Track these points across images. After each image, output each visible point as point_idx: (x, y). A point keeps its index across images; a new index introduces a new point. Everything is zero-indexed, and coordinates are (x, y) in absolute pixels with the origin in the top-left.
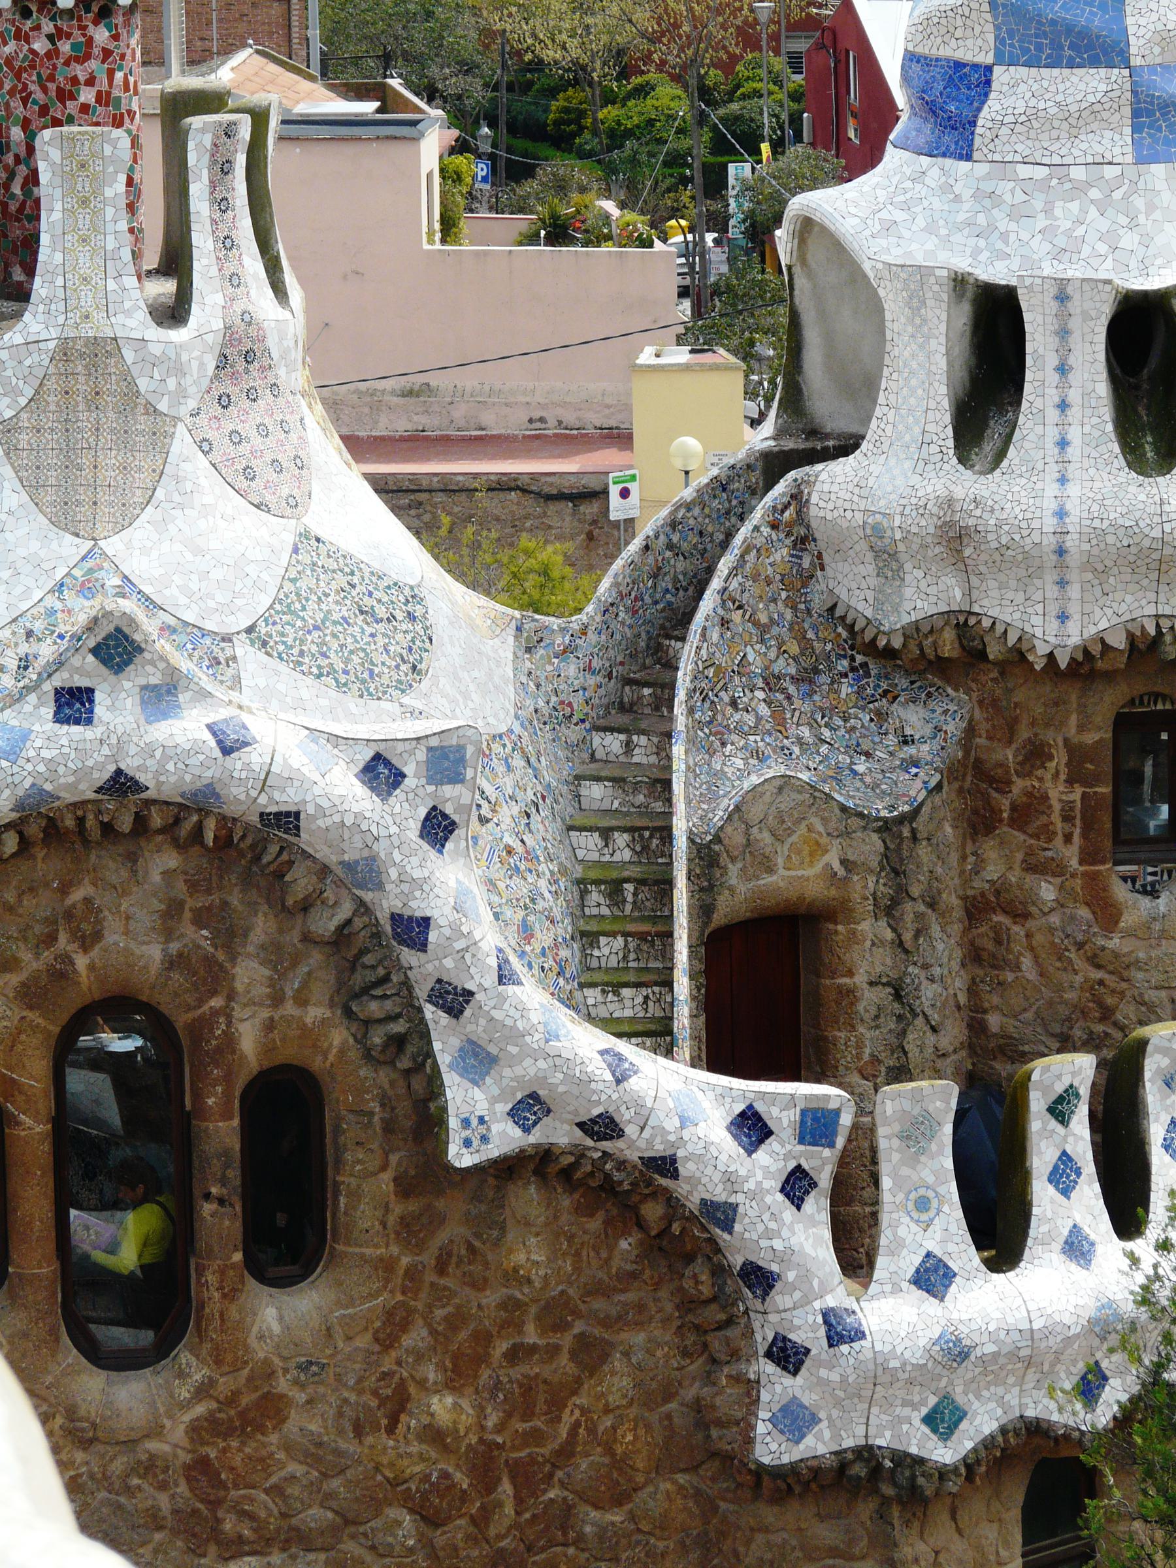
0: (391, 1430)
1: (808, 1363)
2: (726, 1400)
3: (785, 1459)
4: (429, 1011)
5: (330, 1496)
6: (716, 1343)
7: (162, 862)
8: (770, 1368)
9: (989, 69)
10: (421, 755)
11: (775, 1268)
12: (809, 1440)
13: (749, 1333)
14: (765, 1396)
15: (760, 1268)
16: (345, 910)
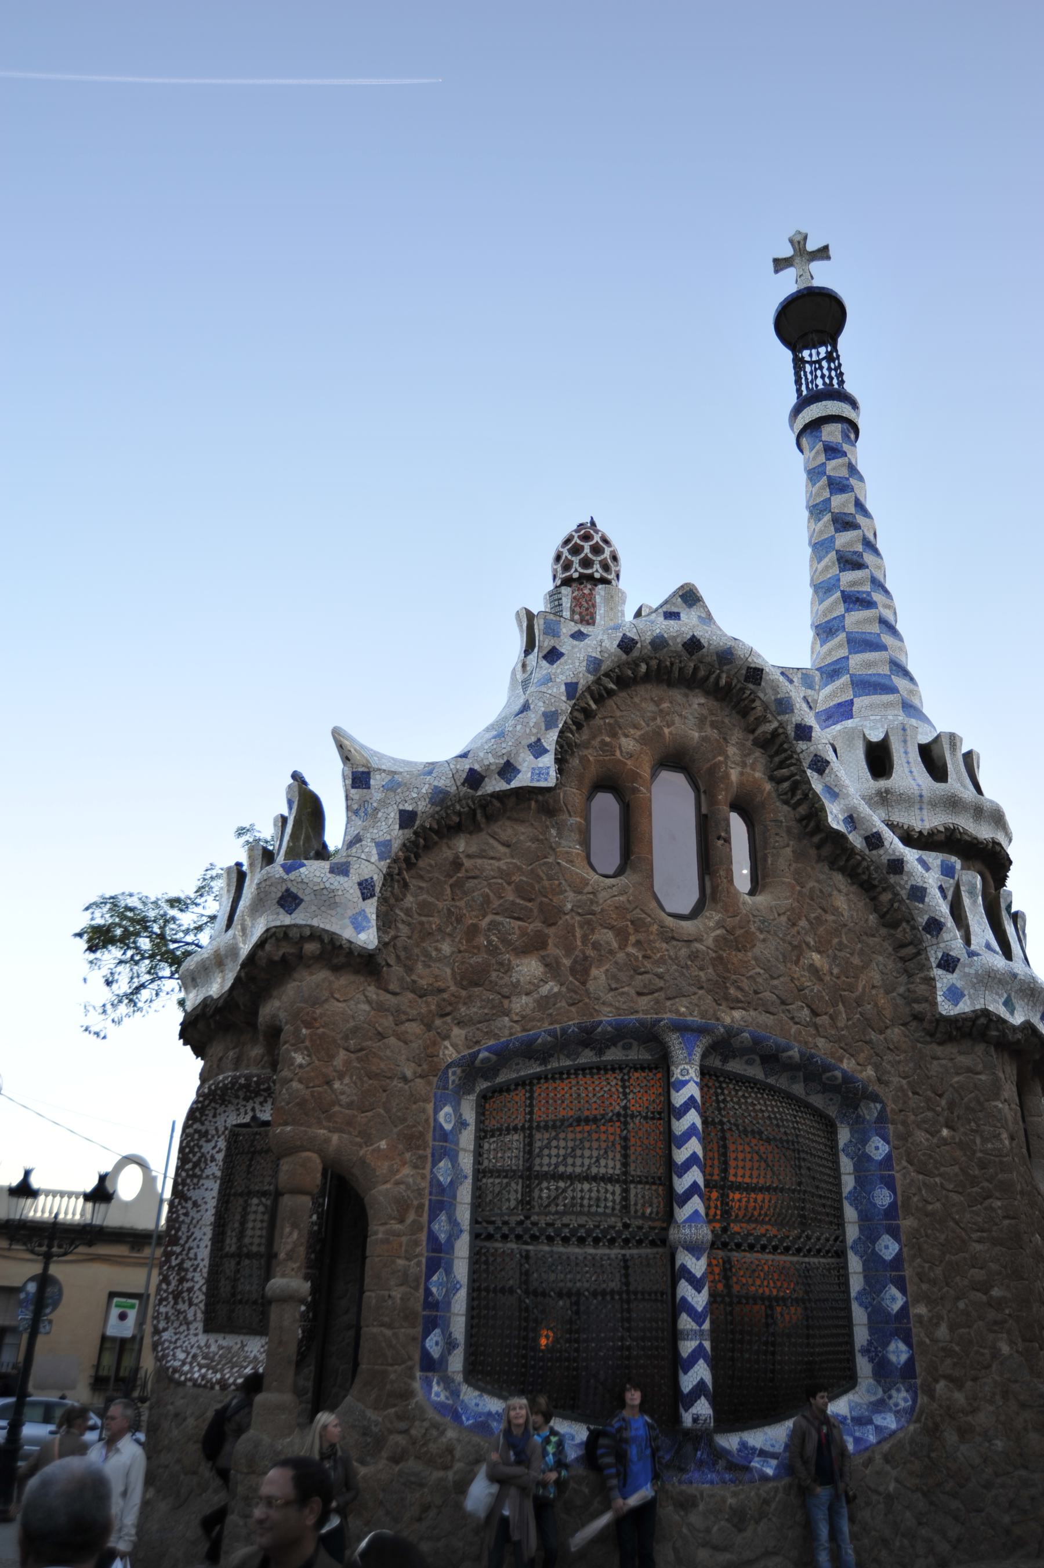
0: (797, 963)
1: (959, 966)
2: (921, 989)
3: (952, 1013)
4: (809, 772)
5: (775, 987)
6: (910, 965)
7: (698, 701)
8: (940, 972)
9: (852, 700)
10: (800, 675)
11: (942, 920)
12: (961, 1005)
13: (928, 959)
14: (939, 985)
15: (936, 920)
16: (775, 724)
